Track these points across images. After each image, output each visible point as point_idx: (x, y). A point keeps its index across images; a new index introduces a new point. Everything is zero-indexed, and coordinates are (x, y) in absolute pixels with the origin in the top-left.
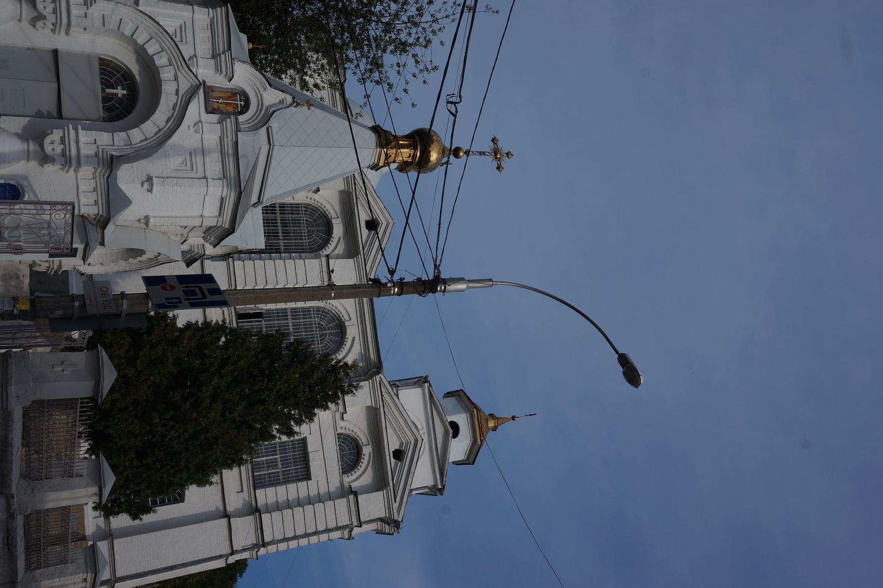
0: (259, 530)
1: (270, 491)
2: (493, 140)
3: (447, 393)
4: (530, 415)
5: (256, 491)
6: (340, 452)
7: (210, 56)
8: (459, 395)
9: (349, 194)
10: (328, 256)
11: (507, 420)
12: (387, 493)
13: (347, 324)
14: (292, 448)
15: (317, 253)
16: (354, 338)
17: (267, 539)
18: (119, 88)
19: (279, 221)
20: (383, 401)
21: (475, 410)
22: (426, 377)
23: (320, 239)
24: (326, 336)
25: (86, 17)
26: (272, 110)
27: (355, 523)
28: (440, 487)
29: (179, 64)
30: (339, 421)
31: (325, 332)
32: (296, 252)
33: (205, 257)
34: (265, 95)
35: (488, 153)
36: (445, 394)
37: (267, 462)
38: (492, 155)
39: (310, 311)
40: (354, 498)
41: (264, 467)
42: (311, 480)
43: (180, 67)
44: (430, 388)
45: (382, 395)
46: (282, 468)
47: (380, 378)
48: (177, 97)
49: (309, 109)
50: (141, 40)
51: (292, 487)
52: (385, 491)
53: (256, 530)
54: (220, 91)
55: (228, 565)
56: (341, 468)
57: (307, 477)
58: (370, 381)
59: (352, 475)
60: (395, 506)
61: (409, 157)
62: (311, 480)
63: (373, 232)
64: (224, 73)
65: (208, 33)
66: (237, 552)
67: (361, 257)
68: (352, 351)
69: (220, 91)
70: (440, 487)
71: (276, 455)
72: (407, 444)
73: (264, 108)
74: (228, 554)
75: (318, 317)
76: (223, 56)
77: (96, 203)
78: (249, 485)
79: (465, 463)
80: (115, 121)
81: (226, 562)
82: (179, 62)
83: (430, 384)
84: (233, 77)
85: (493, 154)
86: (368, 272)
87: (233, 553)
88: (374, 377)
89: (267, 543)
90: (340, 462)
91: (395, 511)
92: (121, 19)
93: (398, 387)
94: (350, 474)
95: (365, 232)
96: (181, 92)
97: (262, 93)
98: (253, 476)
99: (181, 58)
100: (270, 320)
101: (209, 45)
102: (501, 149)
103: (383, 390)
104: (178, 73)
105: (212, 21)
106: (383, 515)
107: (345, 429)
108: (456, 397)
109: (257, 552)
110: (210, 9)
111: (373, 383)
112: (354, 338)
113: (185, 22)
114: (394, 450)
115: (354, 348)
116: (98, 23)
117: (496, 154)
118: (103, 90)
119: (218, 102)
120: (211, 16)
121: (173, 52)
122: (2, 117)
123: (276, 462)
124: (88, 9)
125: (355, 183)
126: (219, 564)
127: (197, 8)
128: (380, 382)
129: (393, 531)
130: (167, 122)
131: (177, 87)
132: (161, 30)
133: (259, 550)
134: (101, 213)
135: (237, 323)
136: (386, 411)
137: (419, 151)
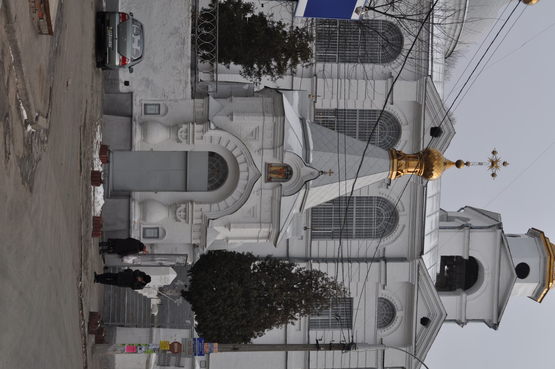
0: (307, 360)
2: (494, 153)
3: (533, 228)
5: (310, 331)
7: (271, 147)
8: (539, 237)
13: (400, 214)
16: (404, 226)
19: (357, 125)
23: (389, 141)
24: (381, 221)
25: (202, 139)
29: (250, 163)
31: (381, 217)
34: (302, 171)
36: (529, 229)
39: (372, 200)
43: (251, 164)
45: (418, 273)
46: (331, 317)
49: (330, 175)
50: (230, 149)
57: (349, 325)
58: (411, 262)
59: (384, 331)
65: (272, 132)
68: (401, 235)
69: (276, 166)
72: (434, 315)
73: (300, 178)
75: (377, 206)
76: (278, 149)
77: (200, 238)
82: (250, 163)
85: (490, 164)
90: (376, 320)
91: (413, 364)
92: (221, 137)
93: (471, 228)
94: (383, 330)
97: (300, 168)
98: (309, 320)
99: (251, 159)
101: (272, 139)
104: (249, 167)
107: (385, 296)
108: (536, 238)
112: (404, 226)
113: (258, 127)
114: (422, 318)
115: (403, 233)
116: (208, 140)
121: (248, 155)
124: (204, 134)
125: (426, 94)
128: (418, 266)
130: (241, 196)
131: (248, 175)
137: (423, 170)
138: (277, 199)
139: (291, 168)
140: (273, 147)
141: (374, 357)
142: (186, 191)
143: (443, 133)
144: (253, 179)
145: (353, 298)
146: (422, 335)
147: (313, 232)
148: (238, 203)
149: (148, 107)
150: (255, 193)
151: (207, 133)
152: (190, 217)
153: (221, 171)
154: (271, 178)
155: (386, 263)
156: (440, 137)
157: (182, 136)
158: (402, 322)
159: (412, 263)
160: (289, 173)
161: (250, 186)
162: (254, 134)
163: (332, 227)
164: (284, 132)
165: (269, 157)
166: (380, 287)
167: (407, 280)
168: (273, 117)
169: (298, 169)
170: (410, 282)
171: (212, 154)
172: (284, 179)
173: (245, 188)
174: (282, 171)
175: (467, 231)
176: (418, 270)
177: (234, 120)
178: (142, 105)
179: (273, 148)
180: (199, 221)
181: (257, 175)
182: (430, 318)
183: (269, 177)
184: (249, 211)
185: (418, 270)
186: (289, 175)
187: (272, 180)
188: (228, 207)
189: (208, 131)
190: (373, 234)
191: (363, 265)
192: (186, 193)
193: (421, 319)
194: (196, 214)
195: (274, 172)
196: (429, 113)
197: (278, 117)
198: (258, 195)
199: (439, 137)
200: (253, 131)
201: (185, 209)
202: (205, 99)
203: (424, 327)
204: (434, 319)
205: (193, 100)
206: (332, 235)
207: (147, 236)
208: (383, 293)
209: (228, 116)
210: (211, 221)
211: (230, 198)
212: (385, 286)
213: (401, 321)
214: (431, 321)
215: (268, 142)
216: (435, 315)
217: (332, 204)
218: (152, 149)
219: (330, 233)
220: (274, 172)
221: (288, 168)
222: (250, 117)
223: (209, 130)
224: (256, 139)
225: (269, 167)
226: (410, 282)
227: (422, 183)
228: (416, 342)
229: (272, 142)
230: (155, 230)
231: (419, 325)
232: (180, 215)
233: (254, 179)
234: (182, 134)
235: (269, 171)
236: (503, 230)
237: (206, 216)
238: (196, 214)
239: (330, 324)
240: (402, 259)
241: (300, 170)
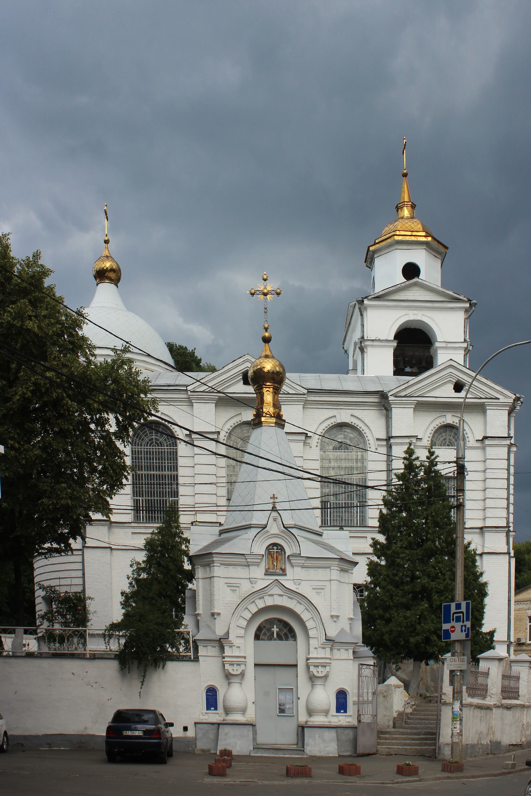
7: (247, 568)
18: (273, 629)
28: (467, 305)
45: (404, 397)
58: (392, 406)
65: (231, 567)
70: (467, 305)
82: (262, 593)
88: (390, 402)
96: (281, 593)
101: (239, 568)
104: (268, 594)
105: (222, 564)
111: (395, 404)
118: (275, 640)
119: (276, 566)
120: (219, 565)
121: (256, 595)
130: (301, 604)
157: (233, 670)
162: (233, 587)
165: (258, 572)
167: (413, 409)
168: (214, 566)
170: (414, 406)
173: (292, 599)
179: (249, 566)
180: (328, 650)
184: (318, 593)
187: (283, 568)
194: (321, 653)
197: (213, 561)
198: (299, 584)
201: (315, 666)
215: (240, 572)
224: (239, 587)
226: (414, 406)
232: (322, 672)
238: (321, 653)
240: (388, 418)
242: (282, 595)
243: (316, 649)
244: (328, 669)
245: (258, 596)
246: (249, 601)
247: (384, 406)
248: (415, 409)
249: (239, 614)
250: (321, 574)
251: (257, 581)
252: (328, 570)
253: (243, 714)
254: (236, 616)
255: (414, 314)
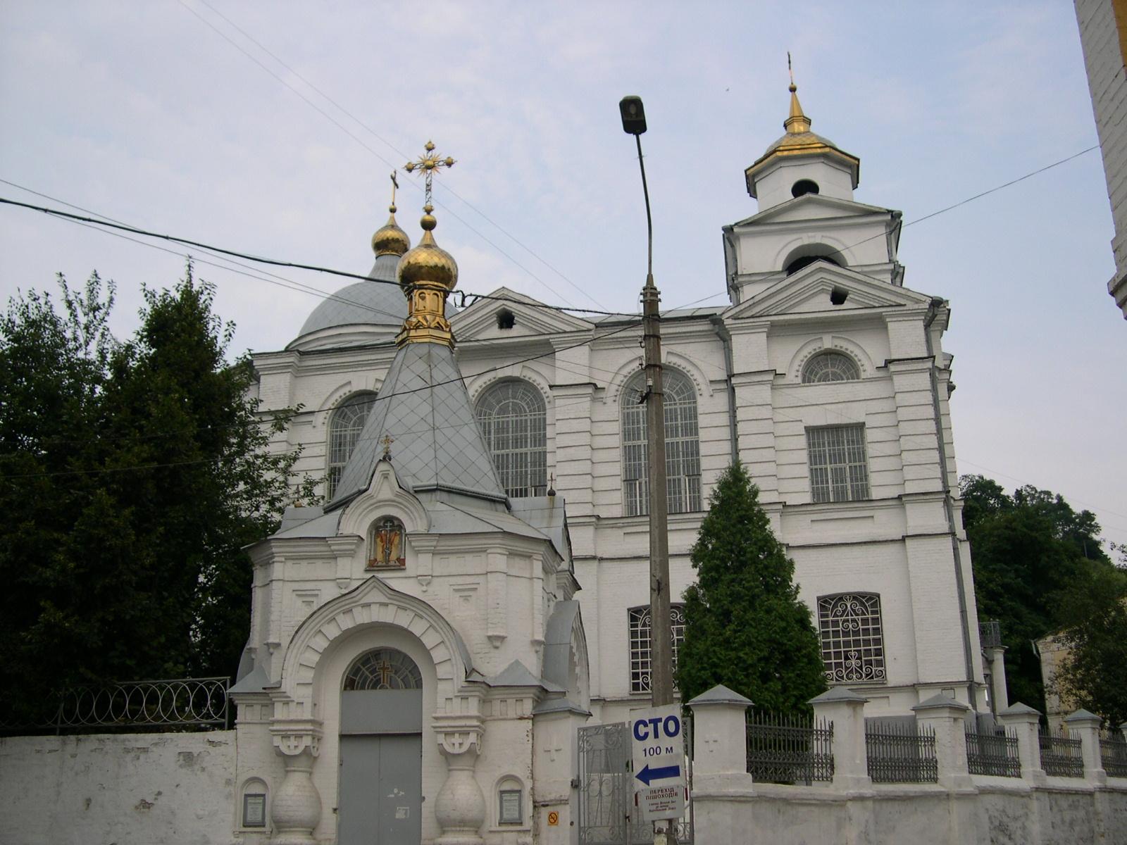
0: (928, 497)
1: (874, 479)
4: (790, 62)
5: (874, 498)
6: (829, 381)
7: (332, 562)
8: (754, 176)
9: (461, 351)
10: (551, 387)
11: (795, 103)
12: (891, 316)
14: (819, 446)
15: (546, 400)
17: (938, 486)
20: (761, 316)
21: (779, 154)
22: (725, 229)
26: (398, 489)
27: (929, 365)
30: (785, 379)
32: (545, 429)
33: (571, 569)
35: (427, 178)
36: (751, 196)
37: (835, 481)
38: (431, 173)
40: (894, 365)
41: (842, 487)
42: (864, 423)
43: (354, 599)
44: (741, 224)
45: (752, 317)
47: (727, 318)
48: (390, 605)
51: (871, 450)
52: (888, 320)
53: (927, 501)
54: (375, 550)
55: (968, 539)
56: (851, 381)
59: (862, 365)
60: (910, 305)
61: (438, 296)
62: (864, 423)
63: (515, 318)
64: (353, 547)
65: (304, 563)
66: (952, 527)
67: (554, 339)
69: (375, 550)
70: (889, 217)
71: (826, 469)
74: (953, 539)
76: (333, 548)
78: (864, 509)
79: (855, 172)
80: (421, 679)
81: (964, 541)
82: (351, 601)
83: (736, 224)
84: (359, 536)
85: (429, 171)
86: (575, 330)
87: (953, 534)
89: (944, 487)
94: (861, 368)
95: (516, 331)
97: (375, 500)
98: (853, 501)
100: (640, 470)
101: (319, 563)
102: (421, 158)
103: (745, 315)
104: (361, 602)
106: (921, 324)
109: (955, 500)
110: (275, 559)
111: (734, 329)
113: (294, 591)
114: (832, 303)
116: (308, 691)
117: (429, 167)
122: (423, 795)
123: (836, 469)
126: (965, 550)
127: (275, 575)
128: (735, 319)
129: (944, 309)
130: (421, 617)
132: (311, 620)
133: (952, 497)
134: (532, 695)
135: (641, 516)
136: (773, 313)
138: (434, 543)
139: (379, 519)
140: (334, 558)
141: (909, 376)
142: (420, 735)
143: (506, 307)
144: (381, 591)
145: (805, 427)
146: (863, 298)
147: (689, 511)
148: (435, 622)
149: (249, 818)
150: (424, 588)
151: (288, 694)
152: (462, 723)
153: (384, 663)
154: (398, 559)
155: (734, 375)
156: (512, 312)
157: (289, 746)
158: (843, 336)
159: (732, 331)
160: (389, 524)
161: (398, 598)
163: (679, 480)
164: (300, 538)
166: (781, 381)
167: (765, 335)
168: (273, 562)
169: (378, 504)
170: (766, 330)
171: (350, 684)
172: (401, 533)
173: (405, 609)
174: (384, 538)
175: (740, 279)
176: (742, 318)
177: (277, 641)
178: (244, 832)
179: (336, 558)
181: (378, 586)
182: (831, 289)
183: (397, 563)
184: (466, 598)
185: (742, 318)
186: (393, 523)
188: (443, 642)
189: (285, 692)
190: (687, 406)
191: (740, 415)
192: (423, 734)
193: (834, 304)
195: (387, 555)
196: (478, 332)
197: (273, 553)
198: (429, 584)
199: (513, 314)
200: (303, 602)
201: (446, 734)
202: (236, 702)
203: (848, 298)
204: (830, 282)
205: (238, 727)
206: (694, 477)
207: (516, 815)
208: (794, 376)
209: (272, 654)
210: (475, 677)
211: (425, 640)
212: (777, 373)
213: (850, 341)
214: (836, 286)
215: (320, 569)
216: (822, 280)
217: (637, 482)
218: (335, 810)
219: (689, 480)
220: (387, 555)
221: (381, 527)
222: (273, 609)
223: (283, 689)
224: (317, 595)
225: (376, 564)
227: (589, 330)
228: (874, 307)
229: (324, 561)
230: (504, 798)
231: (847, 305)
233: (381, 589)
234: (292, 747)
235: (384, 564)
236: (733, 224)
237: (459, 687)
238: (457, 708)
239: (858, 464)
241: (380, 502)
242: (386, 605)
243: (449, 702)
244: (472, 738)
245: (341, 607)
246: (324, 618)
247: (717, 334)
248: (769, 336)
249: (303, 642)
250: (471, 564)
251: (349, 583)
252: (483, 555)
253: (311, 834)
254: (297, 645)
255: (809, 237)
